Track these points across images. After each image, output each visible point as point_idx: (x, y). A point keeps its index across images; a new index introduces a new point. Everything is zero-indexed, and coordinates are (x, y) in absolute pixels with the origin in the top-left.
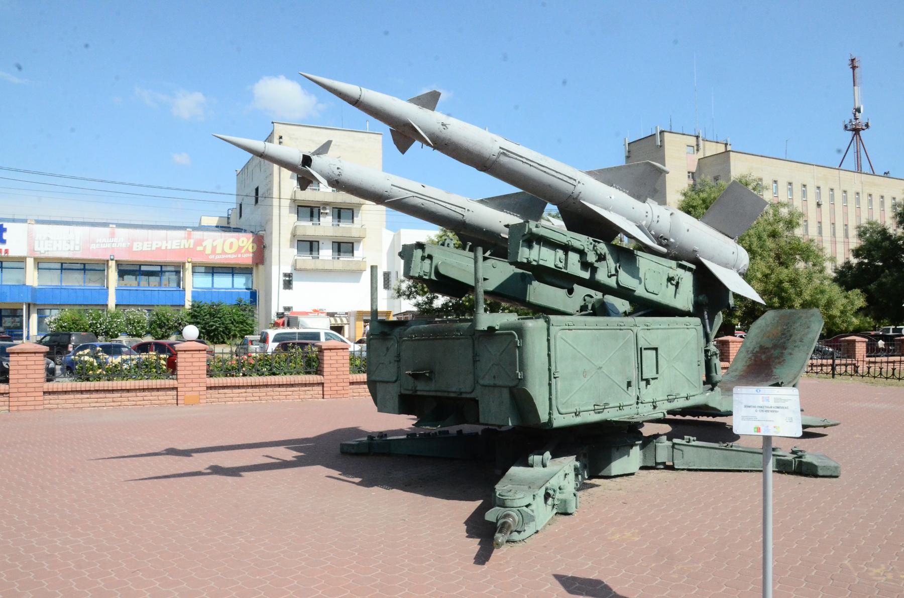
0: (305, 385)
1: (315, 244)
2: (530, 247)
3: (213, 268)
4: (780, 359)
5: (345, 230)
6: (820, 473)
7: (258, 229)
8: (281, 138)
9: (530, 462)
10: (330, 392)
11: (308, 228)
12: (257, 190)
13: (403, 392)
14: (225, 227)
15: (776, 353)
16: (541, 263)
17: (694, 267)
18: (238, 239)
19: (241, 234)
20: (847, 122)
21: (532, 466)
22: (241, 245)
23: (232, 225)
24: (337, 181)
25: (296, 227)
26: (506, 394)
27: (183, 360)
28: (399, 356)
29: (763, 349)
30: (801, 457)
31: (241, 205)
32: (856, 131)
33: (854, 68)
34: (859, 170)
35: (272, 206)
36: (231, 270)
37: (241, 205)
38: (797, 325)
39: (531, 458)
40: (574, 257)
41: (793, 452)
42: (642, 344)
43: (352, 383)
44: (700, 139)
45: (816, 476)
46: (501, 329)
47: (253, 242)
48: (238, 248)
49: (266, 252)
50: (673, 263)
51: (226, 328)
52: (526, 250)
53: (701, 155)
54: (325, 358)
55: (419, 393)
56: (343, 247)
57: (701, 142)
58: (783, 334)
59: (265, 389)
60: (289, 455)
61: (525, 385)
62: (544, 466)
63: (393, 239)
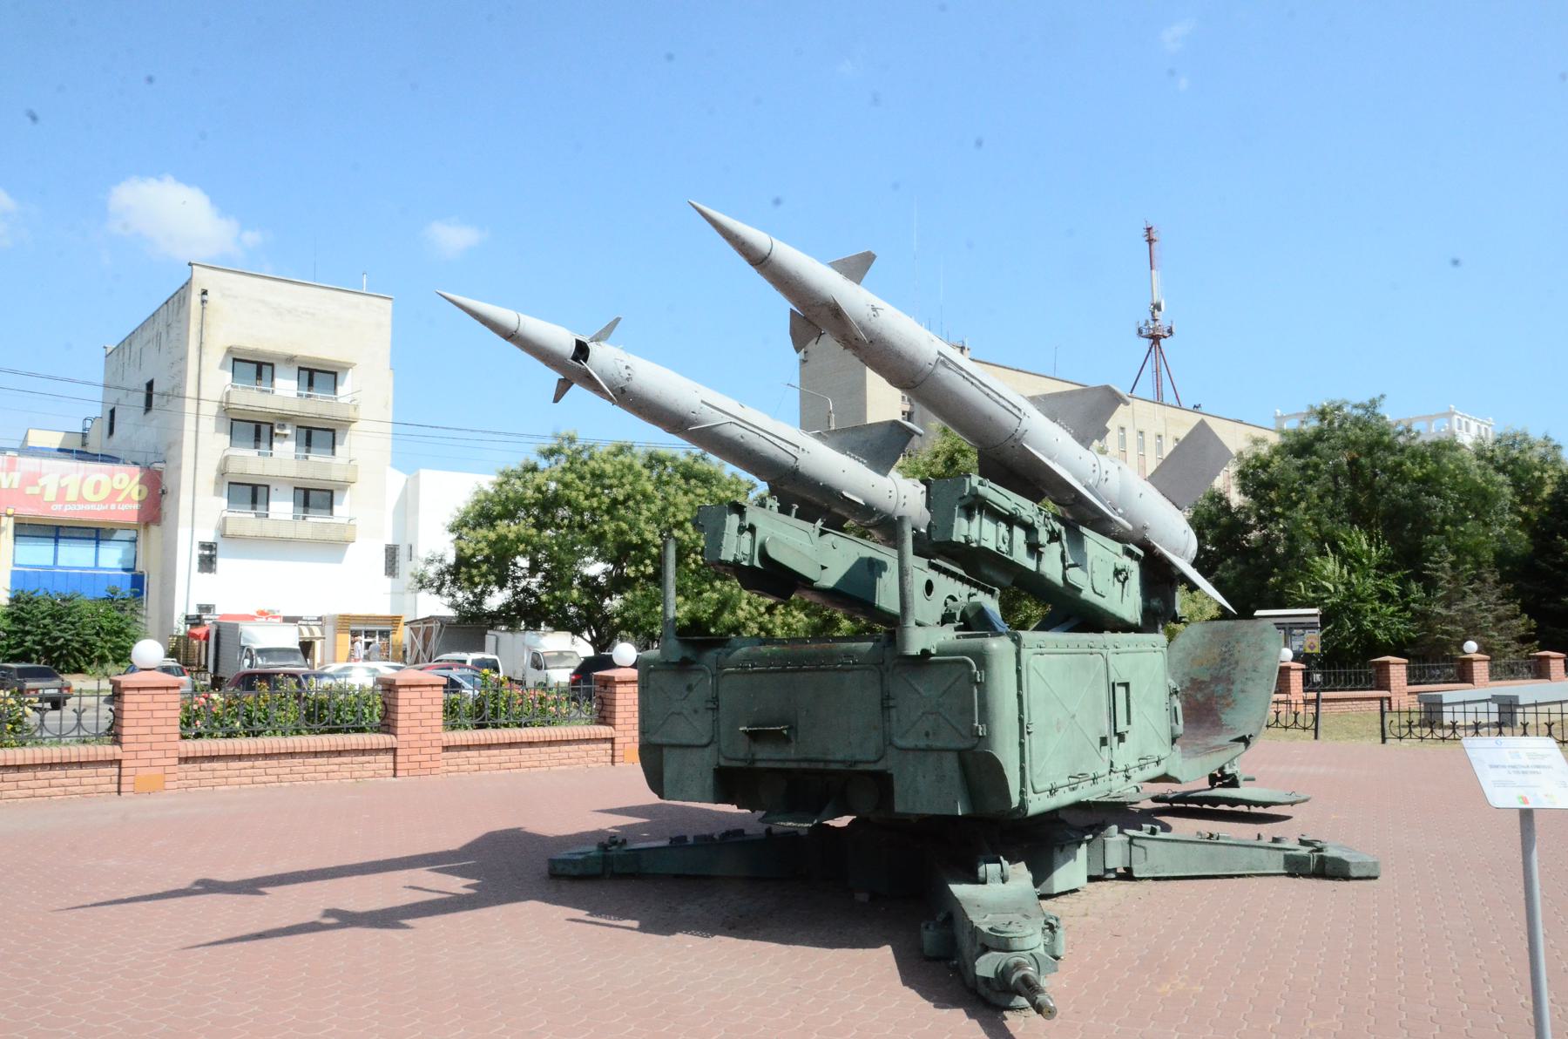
0: (364, 752)
1: (261, 492)
2: (969, 517)
3: (58, 528)
4: (1227, 700)
6: (1354, 873)
7: (151, 458)
8: (205, 293)
9: (981, 875)
10: (408, 766)
11: (251, 462)
12: (150, 385)
13: (723, 763)
14: (81, 453)
15: (1219, 689)
16: (983, 544)
17: (1141, 553)
18: (112, 476)
19: (117, 467)
20: (1142, 324)
21: (984, 882)
22: (117, 486)
23: (93, 448)
24: (623, 390)
25: (226, 458)
26: (951, 764)
27: (134, 707)
28: (716, 699)
29: (1196, 684)
30: (1320, 850)
31: (112, 412)
32: (1155, 339)
33: (1150, 241)
34: (1159, 400)
35: (182, 413)
36: (97, 534)
37: (112, 412)
38: (1243, 645)
39: (981, 869)
40: (1019, 534)
41: (1303, 843)
42: (1114, 678)
43: (446, 748)
45: (1347, 878)
46: (939, 653)
47: (141, 482)
48: (109, 490)
49: (167, 503)
50: (1118, 547)
51: (85, 643)
52: (964, 521)
54: (400, 702)
55: (759, 765)
56: (314, 498)
58: (1223, 660)
59: (290, 761)
60: (457, 885)
61: (988, 746)
62: (1004, 880)
63: (405, 489)
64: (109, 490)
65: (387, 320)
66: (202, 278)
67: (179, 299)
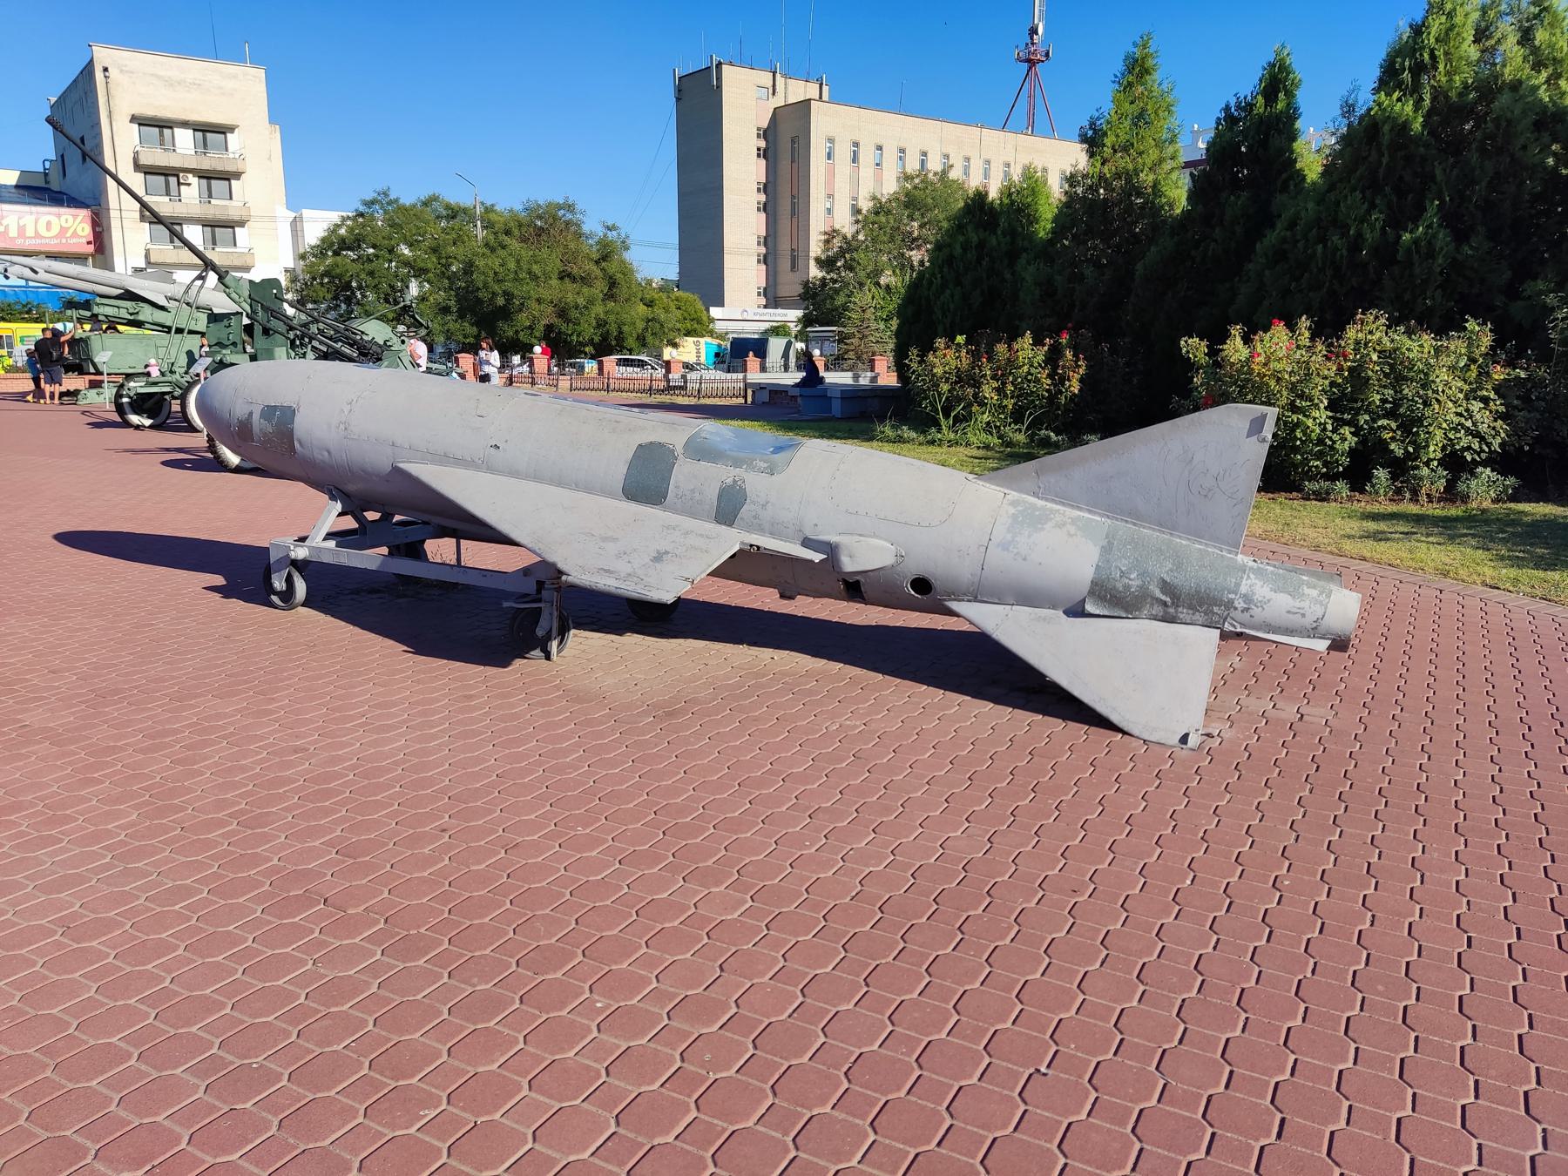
5: (220, 207)
8: (106, 70)
14: (36, 191)
32: (1031, 63)
44: (778, 76)
53: (779, 101)
57: (780, 80)
64: (71, 225)
65: (261, 88)
66: (103, 55)
67: (88, 71)
